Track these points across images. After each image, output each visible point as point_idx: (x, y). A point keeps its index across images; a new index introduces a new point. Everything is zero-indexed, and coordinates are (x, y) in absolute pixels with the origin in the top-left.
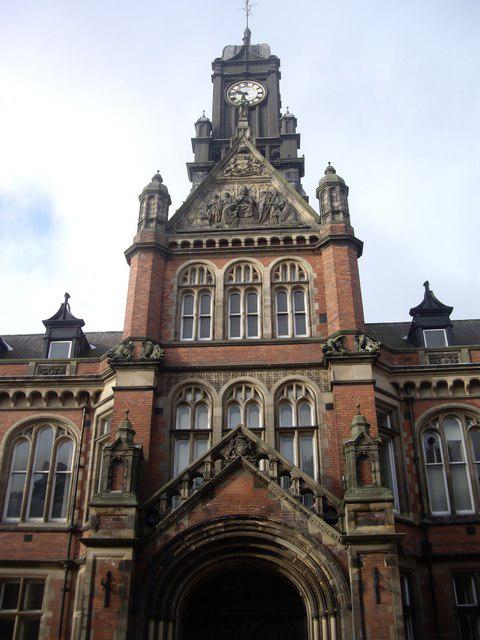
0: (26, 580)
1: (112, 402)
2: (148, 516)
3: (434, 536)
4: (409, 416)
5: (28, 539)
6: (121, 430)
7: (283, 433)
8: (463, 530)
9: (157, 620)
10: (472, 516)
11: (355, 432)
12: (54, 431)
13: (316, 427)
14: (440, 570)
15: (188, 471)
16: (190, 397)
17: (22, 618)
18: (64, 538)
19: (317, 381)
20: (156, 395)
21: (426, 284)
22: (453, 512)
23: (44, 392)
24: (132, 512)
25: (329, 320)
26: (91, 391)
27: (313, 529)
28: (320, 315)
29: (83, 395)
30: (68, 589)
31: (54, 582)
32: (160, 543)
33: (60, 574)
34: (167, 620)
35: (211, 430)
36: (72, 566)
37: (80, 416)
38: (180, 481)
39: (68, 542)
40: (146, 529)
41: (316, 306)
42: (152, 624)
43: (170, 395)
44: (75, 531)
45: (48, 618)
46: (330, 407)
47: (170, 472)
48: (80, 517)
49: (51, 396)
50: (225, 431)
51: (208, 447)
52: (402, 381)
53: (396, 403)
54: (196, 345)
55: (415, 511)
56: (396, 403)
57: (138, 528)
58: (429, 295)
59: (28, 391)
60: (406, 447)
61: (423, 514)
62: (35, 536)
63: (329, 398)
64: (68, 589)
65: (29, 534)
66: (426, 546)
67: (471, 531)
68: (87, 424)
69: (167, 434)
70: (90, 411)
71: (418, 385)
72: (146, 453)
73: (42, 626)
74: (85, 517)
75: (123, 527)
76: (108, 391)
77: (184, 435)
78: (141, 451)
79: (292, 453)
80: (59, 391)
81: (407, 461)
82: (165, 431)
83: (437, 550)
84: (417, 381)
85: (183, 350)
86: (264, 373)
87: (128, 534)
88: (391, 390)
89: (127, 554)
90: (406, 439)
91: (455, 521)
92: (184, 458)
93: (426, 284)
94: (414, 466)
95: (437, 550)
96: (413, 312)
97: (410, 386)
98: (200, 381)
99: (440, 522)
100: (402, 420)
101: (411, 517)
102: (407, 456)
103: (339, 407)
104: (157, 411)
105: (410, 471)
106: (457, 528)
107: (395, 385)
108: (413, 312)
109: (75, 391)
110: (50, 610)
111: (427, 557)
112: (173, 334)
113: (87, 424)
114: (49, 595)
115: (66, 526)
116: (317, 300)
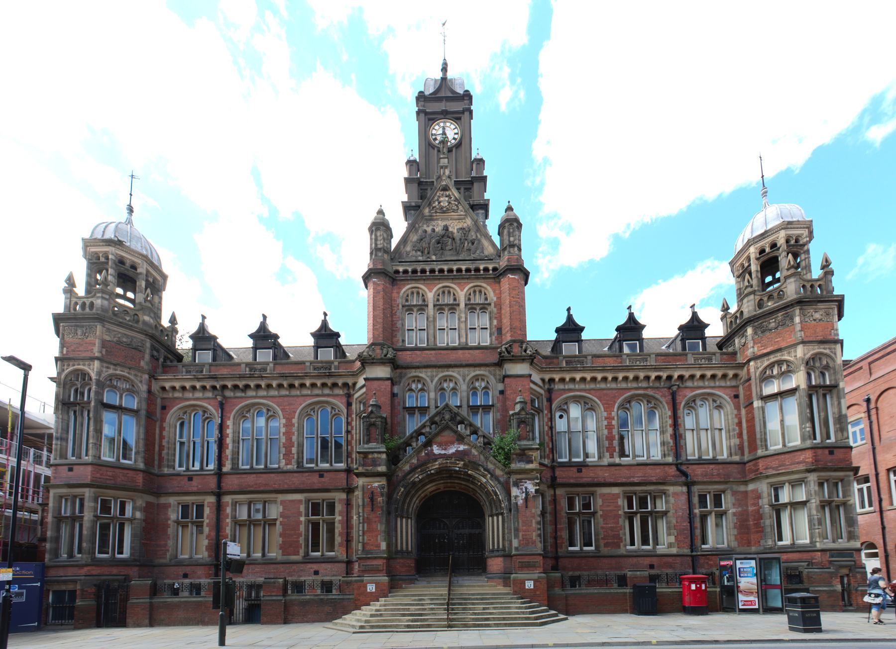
0: (323, 500)
1: (364, 390)
2: (394, 458)
3: (558, 473)
4: (550, 400)
5: (321, 476)
6: (372, 405)
7: (474, 409)
8: (575, 469)
11: (518, 408)
12: (329, 409)
13: (493, 406)
14: (560, 492)
15: (415, 431)
16: (414, 386)
17: (323, 521)
18: (343, 475)
19: (494, 375)
20: (393, 384)
22: (570, 459)
23: (319, 383)
26: (350, 381)
27: (490, 466)
29: (345, 385)
30: (348, 504)
31: (340, 500)
32: (400, 474)
33: (343, 496)
35: (428, 407)
36: (350, 490)
37: (344, 400)
38: (411, 437)
42: (399, 520)
44: (348, 471)
47: (405, 433)
48: (352, 462)
49: (324, 385)
50: (437, 407)
51: (427, 418)
52: (547, 377)
53: (542, 392)
55: (548, 458)
56: (542, 392)
57: (388, 468)
59: (308, 383)
60: (546, 420)
61: (553, 460)
62: (325, 474)
63: (500, 387)
64: (348, 504)
65: (321, 473)
66: (554, 478)
67: (580, 471)
68: (349, 405)
70: (349, 396)
71: (557, 380)
72: (389, 420)
73: (336, 525)
76: (361, 382)
77: (411, 410)
78: (386, 419)
79: (478, 421)
80: (329, 382)
81: (546, 428)
82: (400, 408)
83: (559, 481)
84: (557, 377)
87: (382, 469)
88: (540, 383)
89: (383, 481)
91: (569, 465)
92: (412, 425)
95: (559, 481)
97: (552, 380)
99: (562, 465)
101: (546, 462)
103: (508, 392)
104: (394, 395)
107: (543, 380)
111: (554, 484)
113: (349, 405)
114: (338, 507)
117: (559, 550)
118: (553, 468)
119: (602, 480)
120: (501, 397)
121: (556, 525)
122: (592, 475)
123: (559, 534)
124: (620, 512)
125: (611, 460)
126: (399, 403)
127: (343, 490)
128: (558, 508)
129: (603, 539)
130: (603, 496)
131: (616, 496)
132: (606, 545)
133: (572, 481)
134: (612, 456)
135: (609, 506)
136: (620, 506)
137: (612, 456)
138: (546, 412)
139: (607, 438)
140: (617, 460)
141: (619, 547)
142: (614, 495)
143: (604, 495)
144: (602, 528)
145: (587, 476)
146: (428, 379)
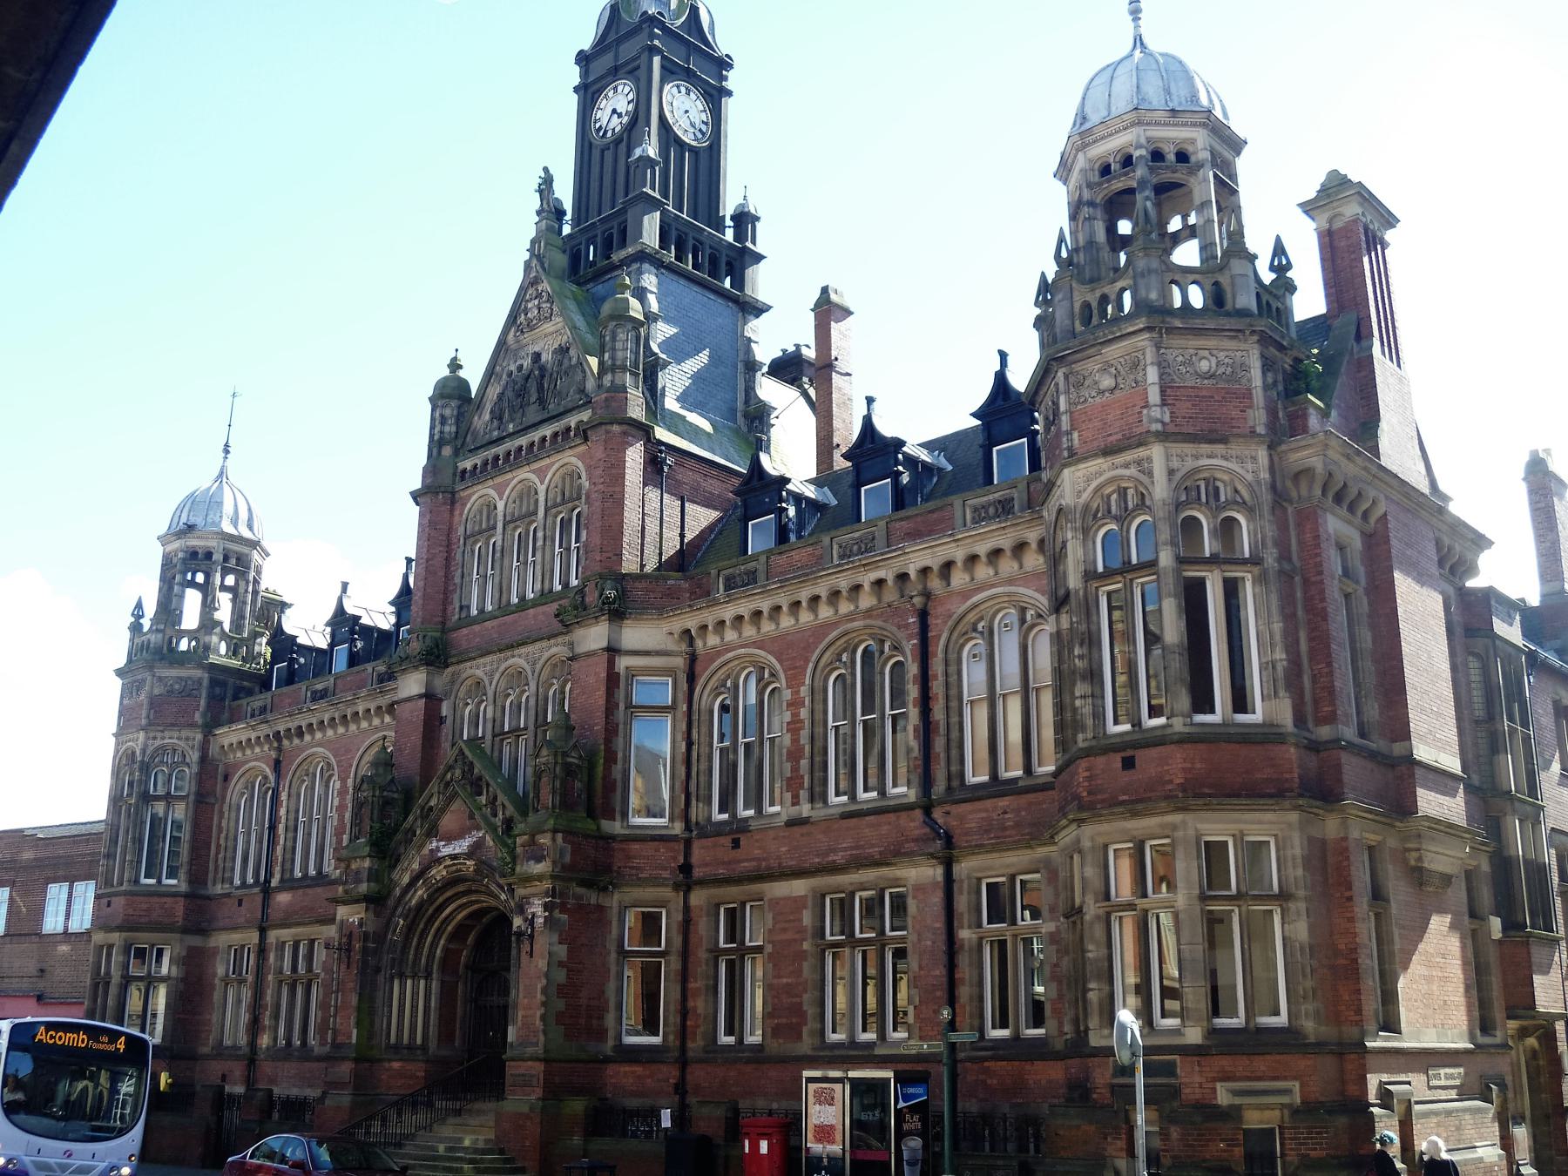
66: (686, 868)
86: (523, 650)
95: (698, 873)
134: (795, 802)
140: (805, 809)
146: (486, 679)
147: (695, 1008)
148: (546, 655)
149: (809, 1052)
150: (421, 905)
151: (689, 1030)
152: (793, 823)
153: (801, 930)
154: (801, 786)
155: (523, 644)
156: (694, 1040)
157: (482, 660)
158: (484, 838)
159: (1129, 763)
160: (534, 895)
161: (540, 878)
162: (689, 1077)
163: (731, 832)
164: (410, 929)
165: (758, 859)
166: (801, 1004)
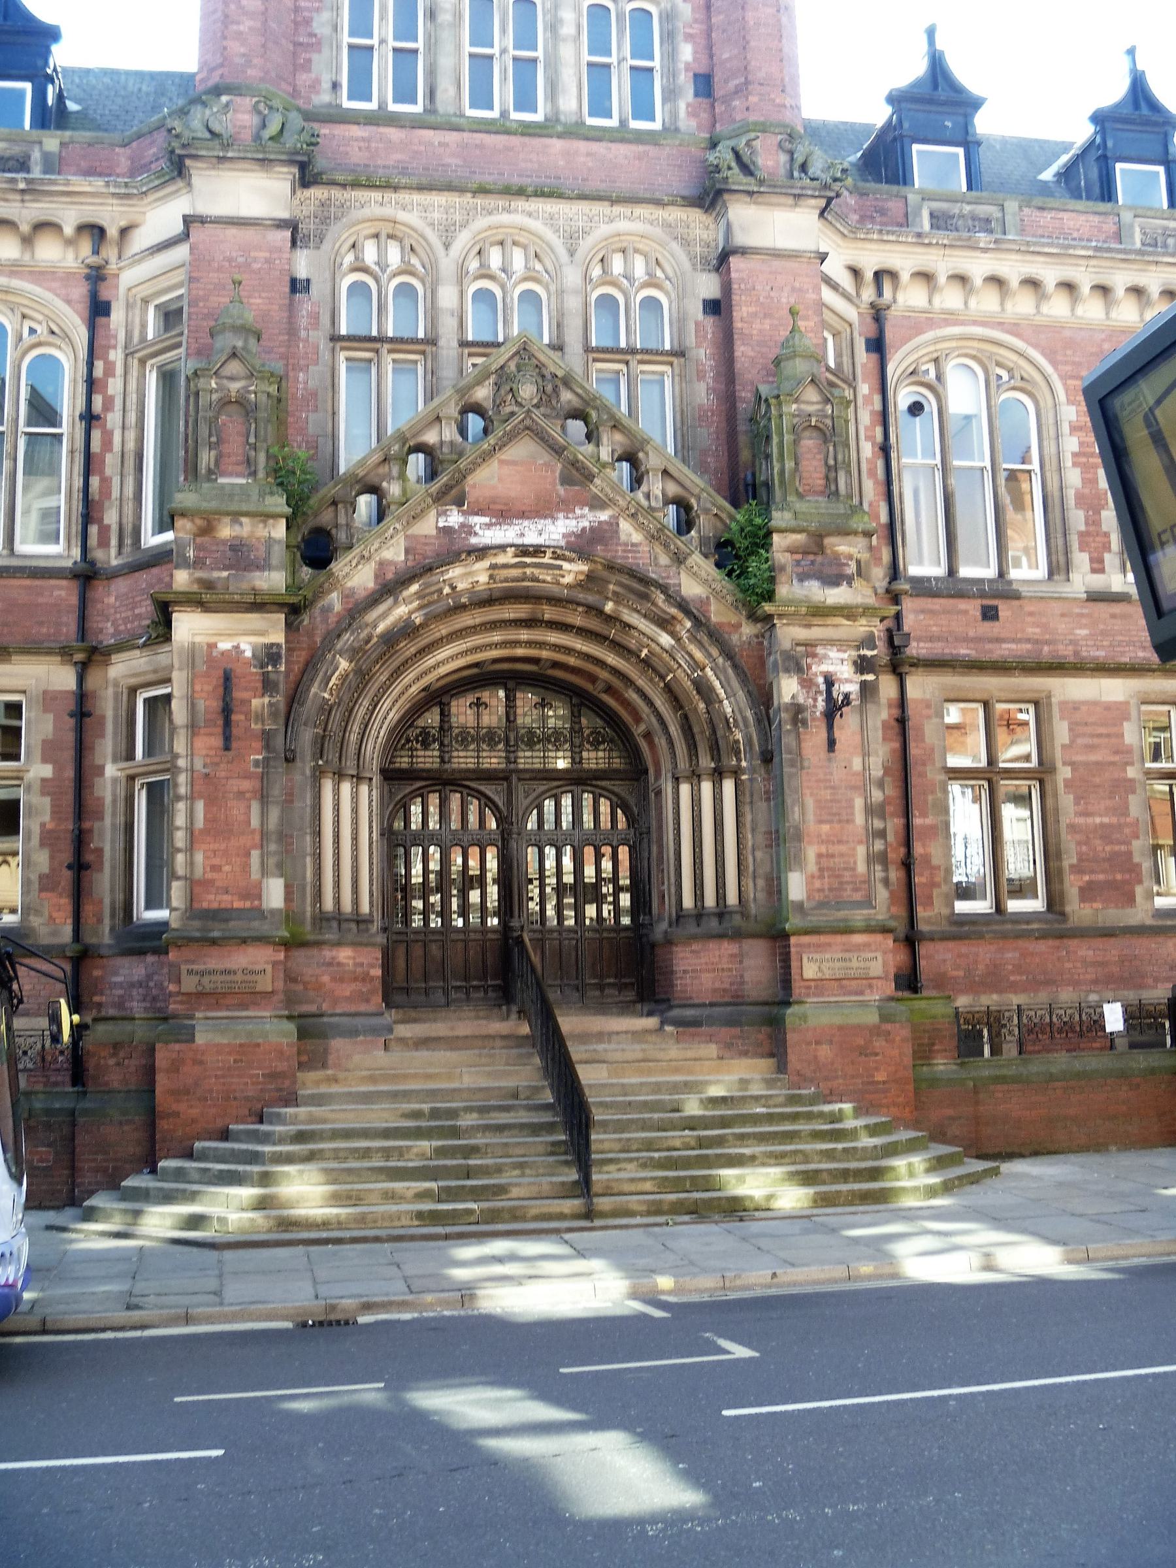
8: (973, 607)
9: (340, 775)
10: (990, 581)
21: (931, 33)
24: (279, 530)
25: (719, 92)
28: (695, 75)
29: (96, 232)
34: (358, 778)
39: (74, 600)
40: (306, 572)
41: (686, 52)
43: (326, 246)
45: (43, 780)
46: (714, 307)
53: (851, 313)
54: (381, 118)
58: (937, 65)
69: (324, 345)
74: (114, 542)
75: (263, 565)
82: (319, 338)
83: (915, 649)
85: (356, 131)
88: (845, 280)
90: (868, 400)
93: (931, 33)
94: (880, 464)
95: (915, 649)
96: (895, 99)
98: (402, 216)
100: (863, 356)
102: (867, 438)
105: (872, 473)
106: (962, 605)
107: (856, 272)
108: (895, 99)
109: (70, 218)
110: (45, 760)
112: (326, 85)
115: (69, 563)
116: (689, 37)
117: (921, 912)
118: (895, 598)
119: (1066, 652)
120: (709, 322)
121: (907, 814)
122: (1032, 631)
123: (918, 849)
124: (1132, 772)
125: (1097, 582)
126: (315, 317)
127: (65, 653)
128: (914, 751)
129: (1077, 869)
130: (1072, 708)
131: (1117, 713)
132: (1087, 893)
133: (964, 651)
135: (1091, 748)
136: (1129, 750)
137: (1098, 567)
138: (864, 389)
139: (1080, 499)
141: (1130, 900)
142: (1108, 707)
143: (1076, 706)
144: (1072, 828)
145: (1013, 634)
147: (927, 859)
148: (604, 229)
149: (1149, 922)
150: (407, 630)
151: (918, 891)
152: (1096, 597)
153: (1123, 751)
154: (1107, 547)
155: (540, 193)
156: (929, 902)
157: (416, 197)
158: (613, 525)
159: (989, 614)
160: (831, 642)
161: (848, 612)
162: (923, 963)
163: (982, 595)
164: (361, 677)
165: (1037, 642)
166: (1129, 854)
